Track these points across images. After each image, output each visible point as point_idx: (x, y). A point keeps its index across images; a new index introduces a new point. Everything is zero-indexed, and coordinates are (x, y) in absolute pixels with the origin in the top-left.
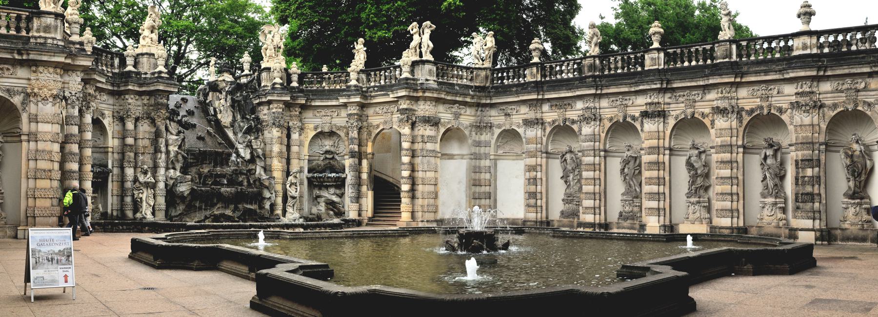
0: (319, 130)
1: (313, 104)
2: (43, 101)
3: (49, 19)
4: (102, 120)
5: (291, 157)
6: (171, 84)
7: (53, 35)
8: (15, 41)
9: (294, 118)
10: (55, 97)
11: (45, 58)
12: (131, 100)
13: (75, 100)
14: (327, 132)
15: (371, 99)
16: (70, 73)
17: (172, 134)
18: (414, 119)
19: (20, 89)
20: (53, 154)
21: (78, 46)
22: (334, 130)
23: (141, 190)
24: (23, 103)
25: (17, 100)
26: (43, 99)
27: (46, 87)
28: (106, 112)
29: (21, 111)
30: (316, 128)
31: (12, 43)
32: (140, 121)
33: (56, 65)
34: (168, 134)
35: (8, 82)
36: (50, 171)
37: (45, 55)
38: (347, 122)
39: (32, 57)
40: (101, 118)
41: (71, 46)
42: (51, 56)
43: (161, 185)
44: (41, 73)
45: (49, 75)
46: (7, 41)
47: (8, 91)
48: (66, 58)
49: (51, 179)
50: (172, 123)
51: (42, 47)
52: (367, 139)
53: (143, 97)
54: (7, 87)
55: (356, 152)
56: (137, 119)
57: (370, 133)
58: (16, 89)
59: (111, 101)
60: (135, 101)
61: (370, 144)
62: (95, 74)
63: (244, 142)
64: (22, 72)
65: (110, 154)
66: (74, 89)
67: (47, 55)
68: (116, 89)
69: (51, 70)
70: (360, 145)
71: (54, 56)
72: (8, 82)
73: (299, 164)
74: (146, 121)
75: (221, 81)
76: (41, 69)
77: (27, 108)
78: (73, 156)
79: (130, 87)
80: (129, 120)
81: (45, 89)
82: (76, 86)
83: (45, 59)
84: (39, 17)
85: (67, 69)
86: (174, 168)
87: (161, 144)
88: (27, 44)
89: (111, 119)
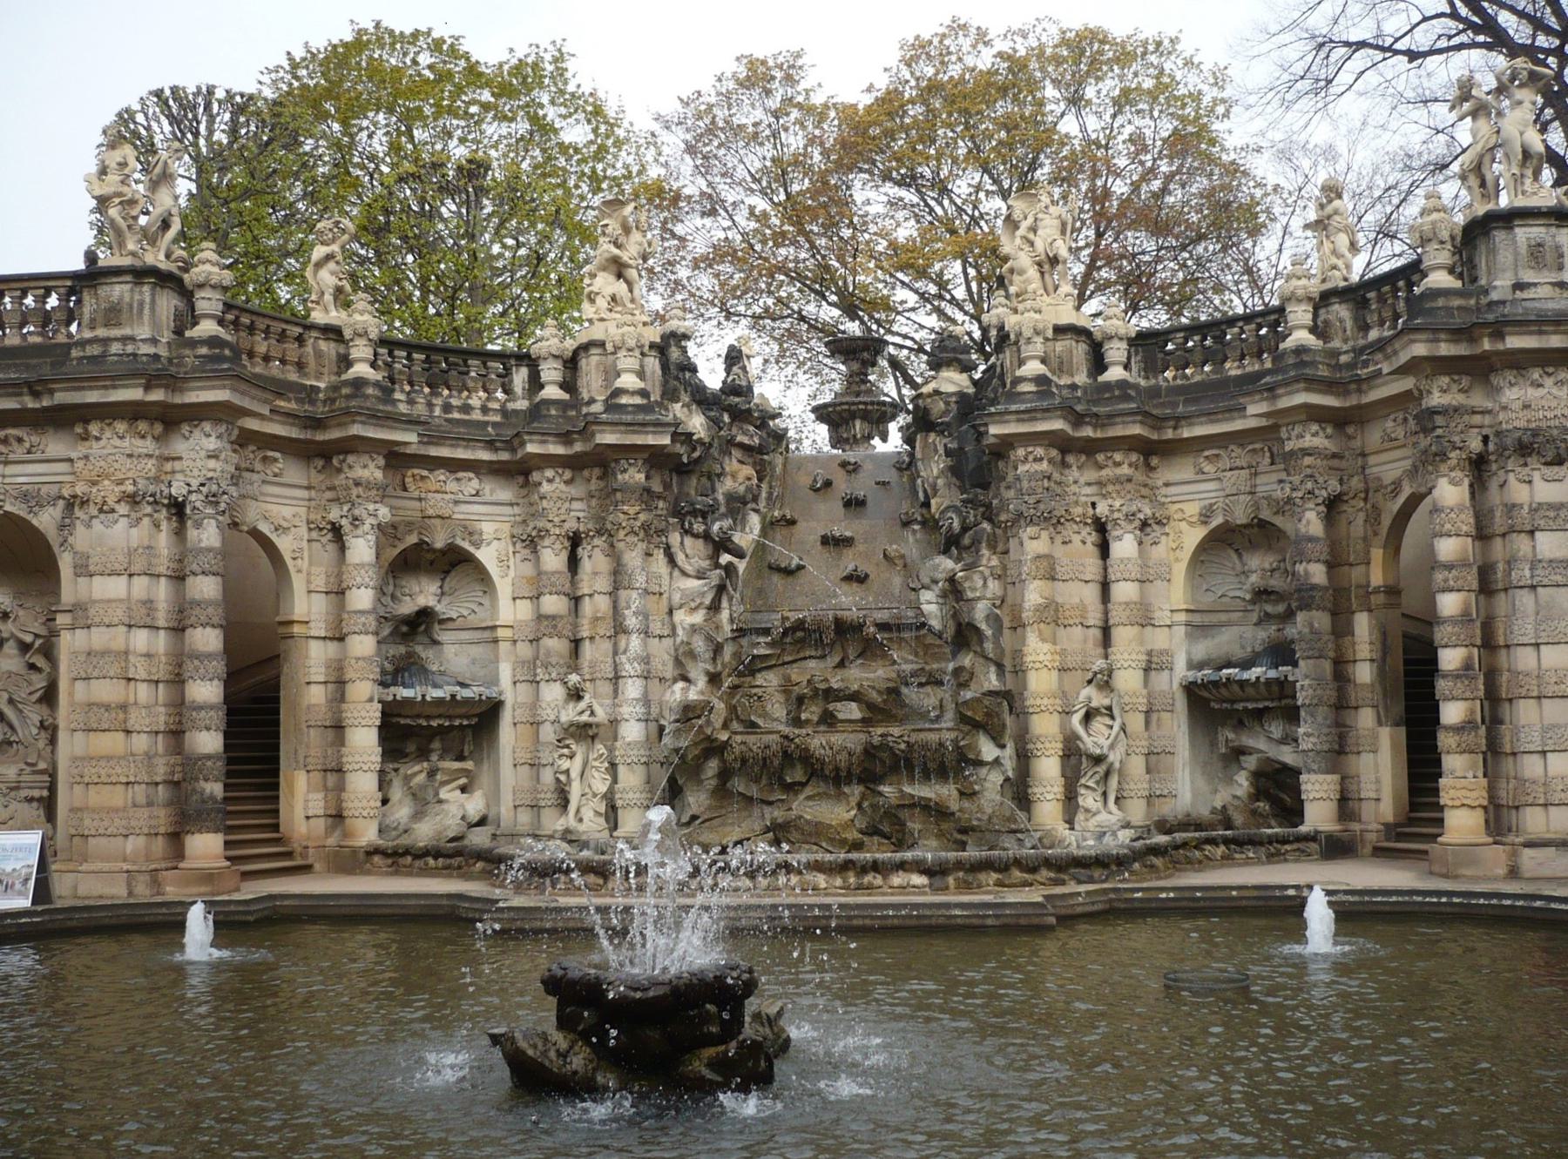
0: (1217, 521)
1: (1186, 433)
2: (102, 516)
3: (117, 288)
4: (471, 549)
5: (1111, 622)
6: (644, 425)
7: (127, 331)
8: (34, 361)
9: (1110, 488)
10: (133, 500)
11: (92, 397)
12: (552, 485)
13: (198, 504)
14: (1245, 526)
15: (1360, 391)
16: (185, 428)
17: (684, 574)
18: (1475, 445)
19: (54, 490)
20: (132, 658)
21: (204, 351)
22: (1266, 514)
23: (568, 747)
24: (62, 527)
25: (46, 520)
26: (101, 511)
27: (107, 477)
28: (488, 528)
29: (56, 549)
30: (1205, 517)
31: (28, 367)
33: (133, 413)
34: (676, 573)
35: (23, 474)
36: (124, 707)
37: (91, 388)
38: (1281, 481)
39: (62, 397)
40: (466, 545)
41: (187, 352)
42: (105, 387)
43: (632, 731)
44: (98, 439)
45: (117, 442)
46: (16, 365)
47: (25, 497)
48: (148, 388)
49: (128, 732)
50: (688, 541)
51: (101, 370)
52: (1365, 539)
53: (586, 473)
54: (25, 487)
55: (1314, 587)
56: (575, 541)
57: (1374, 516)
58: (44, 489)
59: (505, 493)
60: (562, 487)
61: (1377, 554)
62: (354, 422)
63: (935, 582)
64: (56, 445)
65: (504, 647)
66: (196, 472)
67: (97, 388)
68: (505, 456)
69: (121, 427)
70: (1332, 565)
71: (114, 387)
72: (23, 474)
73: (1142, 643)
74: (597, 541)
75: (929, 395)
76: (94, 428)
77: (71, 540)
78: (196, 662)
79: (531, 448)
80: (547, 542)
81: (106, 482)
82: (199, 463)
83: (93, 400)
84: (95, 286)
85: (171, 420)
86: (686, 679)
87: (629, 607)
88: (63, 364)
89: (505, 546)
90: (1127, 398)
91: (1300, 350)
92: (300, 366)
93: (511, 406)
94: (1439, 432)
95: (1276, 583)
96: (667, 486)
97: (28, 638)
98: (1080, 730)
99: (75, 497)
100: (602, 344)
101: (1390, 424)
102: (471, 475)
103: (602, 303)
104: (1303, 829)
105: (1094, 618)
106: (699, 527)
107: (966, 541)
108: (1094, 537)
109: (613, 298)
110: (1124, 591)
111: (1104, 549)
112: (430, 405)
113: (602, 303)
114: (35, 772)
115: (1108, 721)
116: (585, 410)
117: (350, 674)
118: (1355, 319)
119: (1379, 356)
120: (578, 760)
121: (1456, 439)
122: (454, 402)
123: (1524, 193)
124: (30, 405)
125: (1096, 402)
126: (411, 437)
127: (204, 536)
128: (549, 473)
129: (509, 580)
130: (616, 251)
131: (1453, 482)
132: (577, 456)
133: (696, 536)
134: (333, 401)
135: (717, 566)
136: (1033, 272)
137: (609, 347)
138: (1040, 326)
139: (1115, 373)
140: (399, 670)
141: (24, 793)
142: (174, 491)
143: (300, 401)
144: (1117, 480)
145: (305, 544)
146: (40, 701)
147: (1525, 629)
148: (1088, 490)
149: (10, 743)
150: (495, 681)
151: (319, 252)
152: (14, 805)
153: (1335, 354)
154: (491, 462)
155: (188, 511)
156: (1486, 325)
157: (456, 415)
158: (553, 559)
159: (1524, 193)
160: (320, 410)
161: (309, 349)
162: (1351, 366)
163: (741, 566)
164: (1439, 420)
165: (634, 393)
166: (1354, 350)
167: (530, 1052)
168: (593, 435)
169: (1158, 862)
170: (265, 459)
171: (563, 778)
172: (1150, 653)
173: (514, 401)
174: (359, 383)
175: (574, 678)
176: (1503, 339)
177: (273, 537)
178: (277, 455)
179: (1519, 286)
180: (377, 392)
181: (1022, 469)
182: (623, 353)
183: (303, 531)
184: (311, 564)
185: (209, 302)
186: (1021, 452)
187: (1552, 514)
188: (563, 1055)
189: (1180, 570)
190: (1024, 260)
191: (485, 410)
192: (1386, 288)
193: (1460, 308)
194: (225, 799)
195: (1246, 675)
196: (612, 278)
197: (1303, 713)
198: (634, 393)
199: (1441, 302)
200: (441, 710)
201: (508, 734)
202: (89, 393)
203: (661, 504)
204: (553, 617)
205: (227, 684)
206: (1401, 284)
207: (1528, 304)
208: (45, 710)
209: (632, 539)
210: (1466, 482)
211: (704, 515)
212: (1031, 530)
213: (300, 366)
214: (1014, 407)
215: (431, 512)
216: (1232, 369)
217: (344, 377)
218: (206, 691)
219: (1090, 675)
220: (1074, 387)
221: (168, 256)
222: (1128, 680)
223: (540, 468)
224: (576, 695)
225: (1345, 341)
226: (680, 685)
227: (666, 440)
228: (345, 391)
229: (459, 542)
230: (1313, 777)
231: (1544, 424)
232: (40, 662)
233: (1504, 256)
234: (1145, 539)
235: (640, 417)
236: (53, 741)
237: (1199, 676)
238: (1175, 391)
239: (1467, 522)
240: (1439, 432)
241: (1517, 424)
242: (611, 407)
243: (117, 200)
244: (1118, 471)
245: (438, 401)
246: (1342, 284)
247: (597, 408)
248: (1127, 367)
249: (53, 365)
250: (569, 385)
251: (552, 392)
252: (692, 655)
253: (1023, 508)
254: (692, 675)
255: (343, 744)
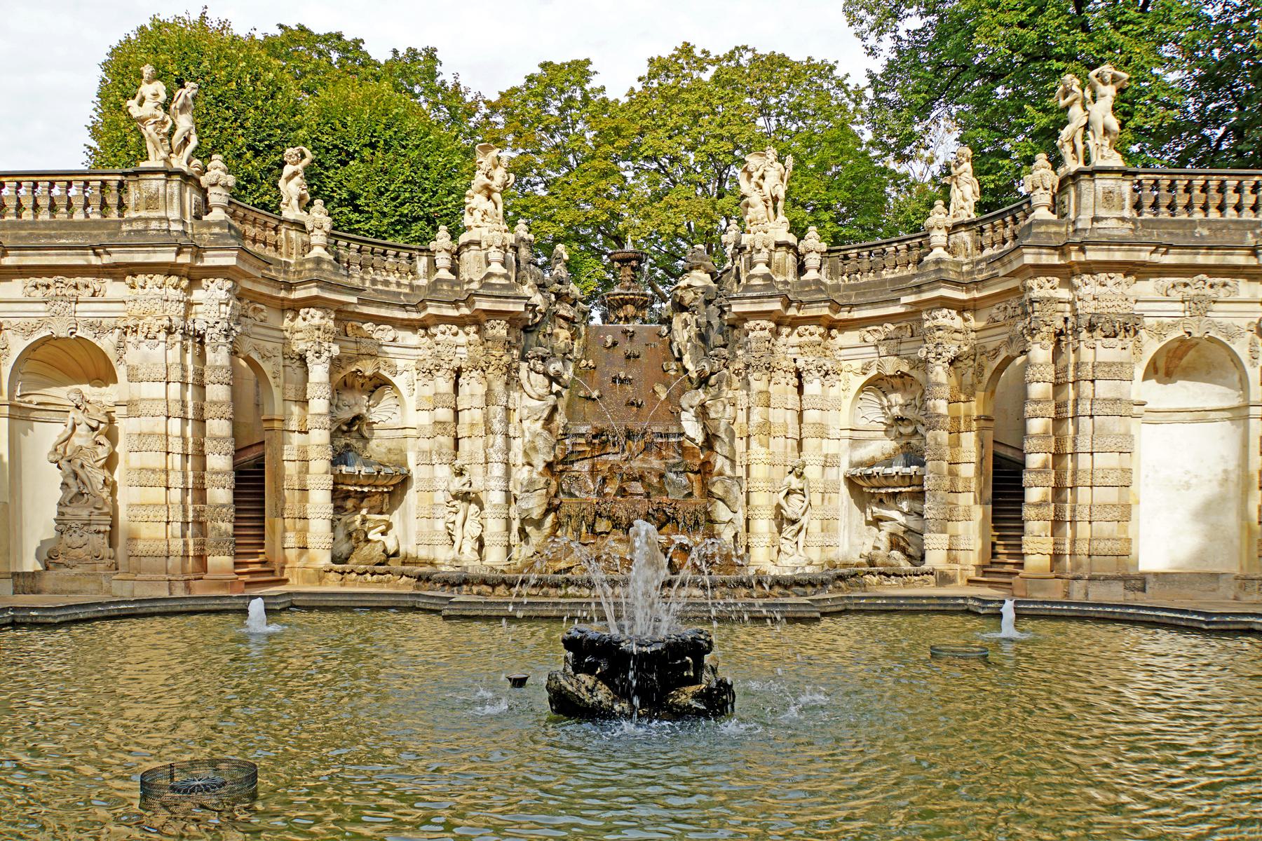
0: (873, 372)
4: (390, 377)
9: (806, 349)
14: (891, 377)
18: (1059, 324)
21: (217, 230)
32: (463, 375)
37: (138, 252)
40: (386, 374)
41: (205, 230)
50: (533, 375)
75: (685, 288)
90: (821, 291)
91: (938, 261)
92: (276, 247)
93: (415, 283)
94: (1036, 314)
95: (909, 414)
96: (518, 340)
97: (94, 424)
98: (783, 503)
99: (127, 327)
100: (479, 244)
101: (995, 311)
102: (389, 327)
103: (478, 215)
104: (926, 567)
105: (793, 432)
106: (540, 367)
107: (713, 380)
108: (796, 381)
109: (485, 213)
110: (810, 416)
111: (800, 389)
112: (363, 279)
113: (478, 215)
114: (101, 514)
115: (801, 497)
116: (466, 287)
117: (311, 455)
118: (975, 242)
119: (998, 264)
120: (461, 515)
121: (1047, 319)
122: (379, 278)
123: (1103, 157)
124: (94, 262)
125: (799, 293)
126: (354, 300)
127: (219, 358)
128: (442, 327)
129: (414, 398)
130: (488, 181)
131: (1043, 348)
132: (462, 317)
133: (538, 373)
134: (300, 272)
135: (551, 393)
136: (761, 206)
137: (484, 245)
138: (766, 242)
139: (811, 275)
140: (339, 458)
141: (93, 528)
142: (197, 327)
143: (278, 271)
144: (811, 344)
145: (281, 368)
146: (103, 467)
147: (1084, 443)
148: (791, 350)
149: (83, 494)
150: (405, 464)
151: (288, 170)
152: (86, 536)
153: (960, 264)
154: (403, 320)
155: (207, 340)
156: (1074, 244)
157: (380, 287)
158: (443, 384)
159: (1103, 157)
160: (292, 279)
161: (282, 235)
162: (970, 273)
163: (564, 392)
164: (1036, 305)
165: (500, 276)
166: (972, 262)
167: (569, 688)
168: (474, 302)
169: (842, 584)
170: (255, 309)
171: (451, 526)
172: (826, 456)
173: (418, 279)
174: (318, 261)
175: (458, 463)
176: (1084, 252)
177: (260, 362)
178: (263, 307)
179: (1095, 219)
180: (330, 268)
181: (751, 334)
182: (493, 248)
183: (280, 359)
184: (285, 382)
185: (217, 197)
186: (751, 324)
187: (1107, 369)
188: (590, 691)
189: (846, 404)
190: (755, 198)
191: (399, 284)
192: (997, 222)
193: (1055, 233)
194: (234, 535)
195: (888, 471)
196: (484, 199)
197: (927, 495)
198: (500, 276)
199: (1043, 229)
200: (370, 482)
201: (412, 496)
202: (136, 255)
203: (515, 352)
204: (444, 423)
205: (234, 458)
206: (1008, 219)
207: (1101, 231)
208: (107, 473)
209: (498, 372)
210: (1052, 347)
211: (543, 359)
212: (757, 375)
213: (276, 247)
214: (749, 295)
215: (363, 351)
216: (887, 274)
217: (307, 256)
218: (219, 462)
219: (789, 469)
220: (786, 283)
221: (188, 163)
222: (812, 472)
223: (436, 325)
224: (460, 473)
225: (967, 256)
226: (527, 468)
227: (522, 308)
228: (308, 266)
229: (381, 371)
230: (932, 535)
231: (1105, 311)
232: (102, 439)
233: (1087, 200)
234: (827, 383)
235: (505, 293)
236: (113, 493)
237: (858, 472)
238: (848, 287)
239: (1050, 373)
240: (1036, 314)
241: (1088, 310)
242: (484, 285)
243: (153, 120)
244: (812, 338)
245: (368, 277)
246: (967, 219)
247: (475, 286)
248: (819, 270)
249: (109, 235)
250: (454, 270)
251: (444, 274)
252: (535, 449)
253: (752, 360)
254: (534, 463)
255: (307, 501)
